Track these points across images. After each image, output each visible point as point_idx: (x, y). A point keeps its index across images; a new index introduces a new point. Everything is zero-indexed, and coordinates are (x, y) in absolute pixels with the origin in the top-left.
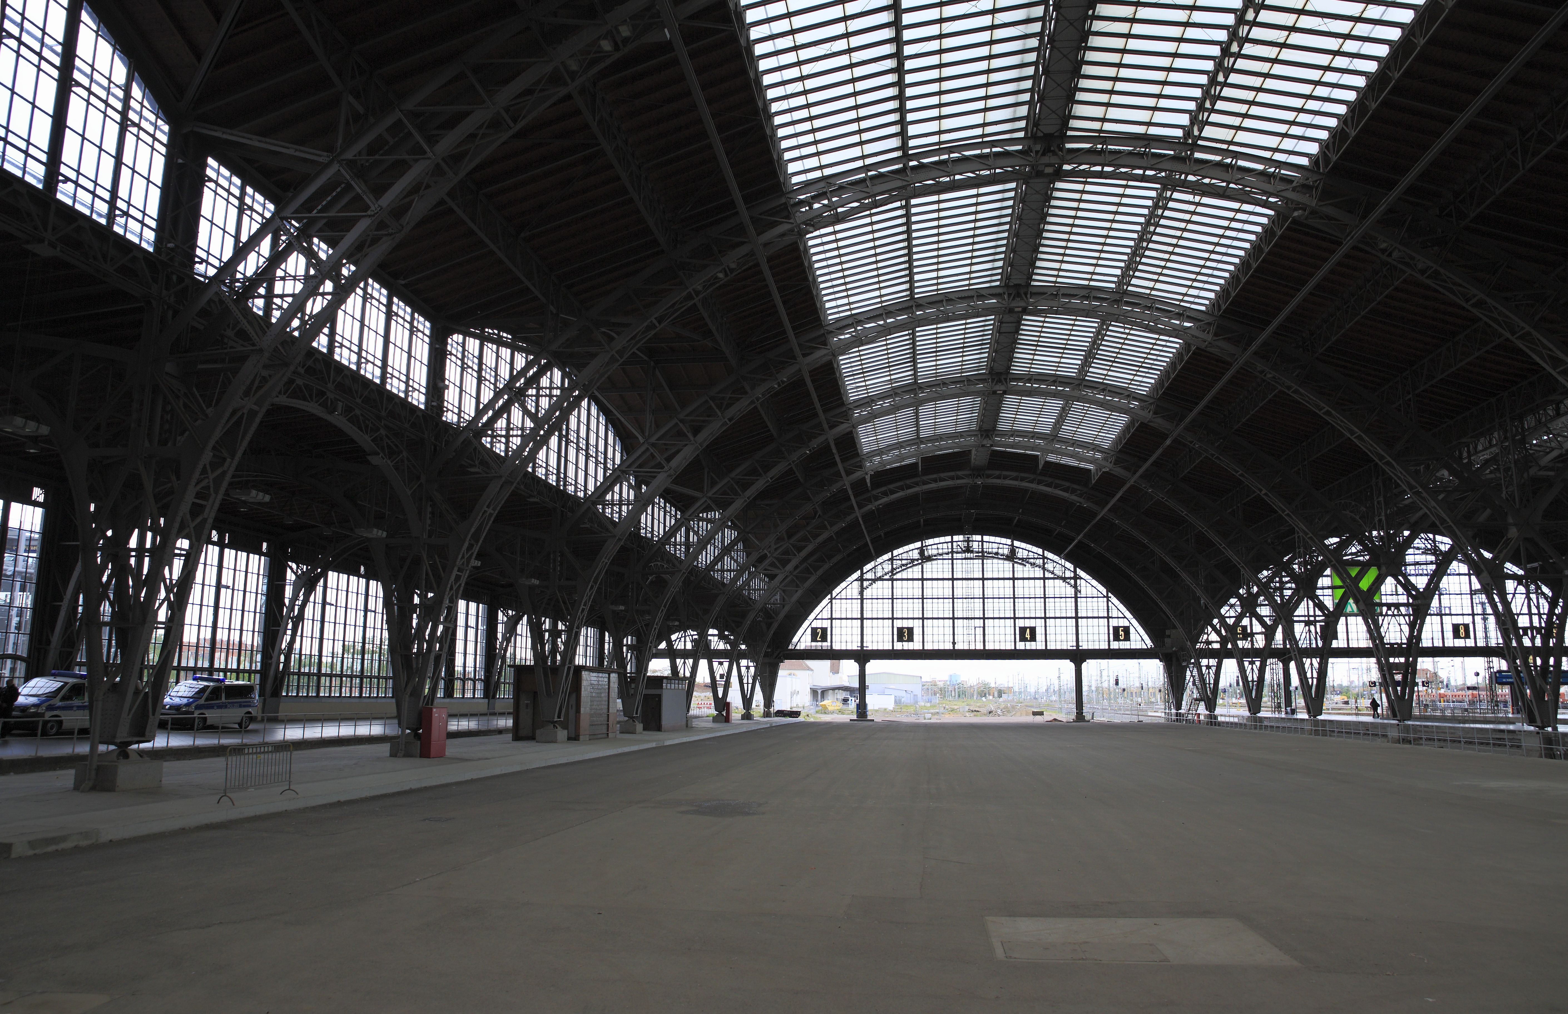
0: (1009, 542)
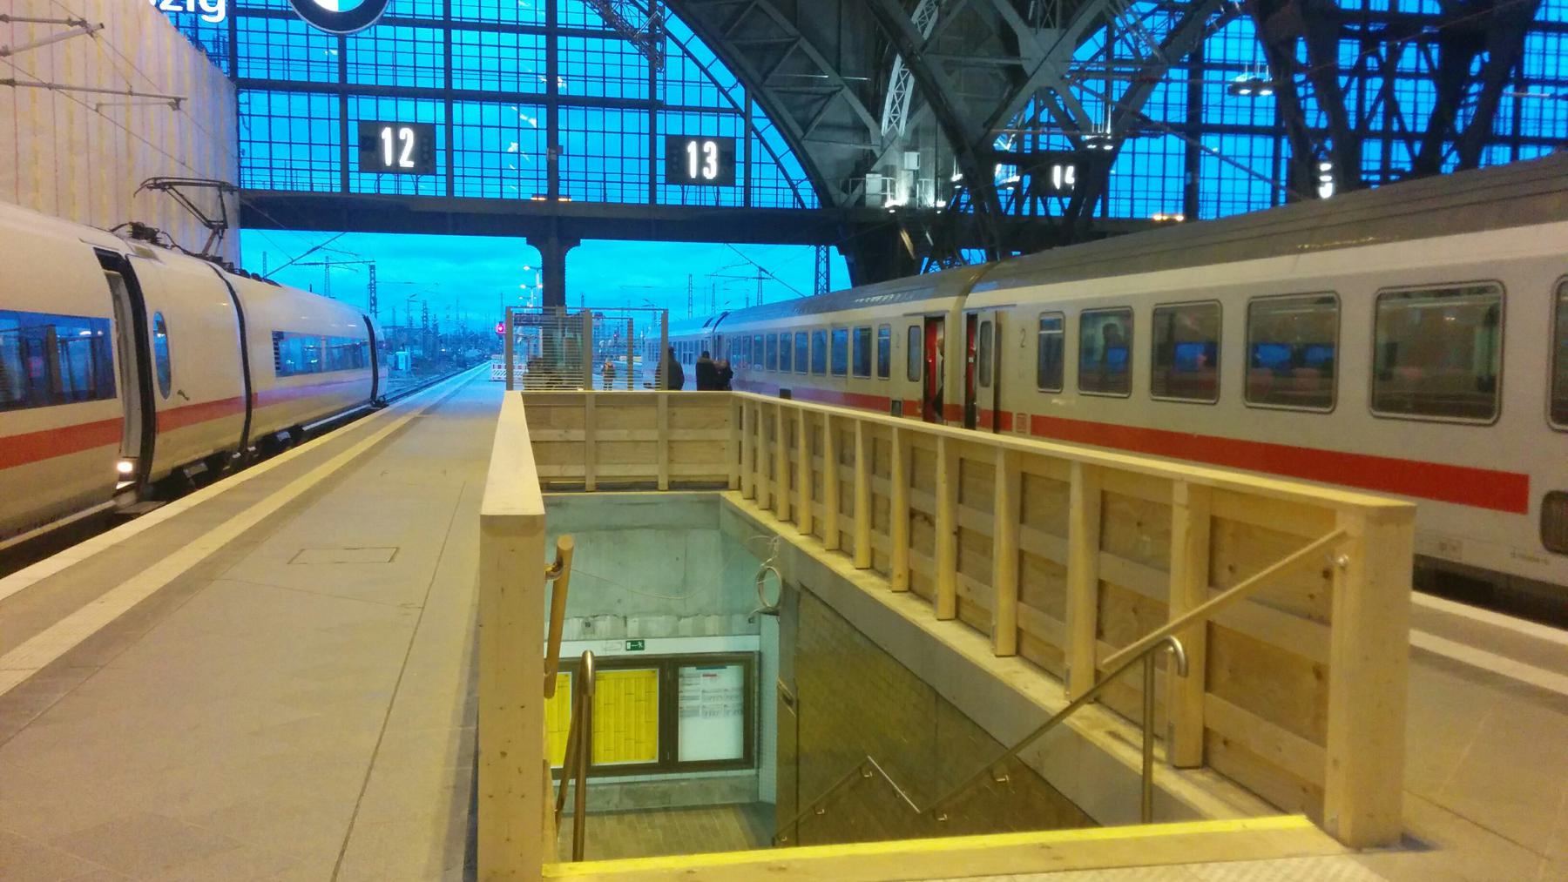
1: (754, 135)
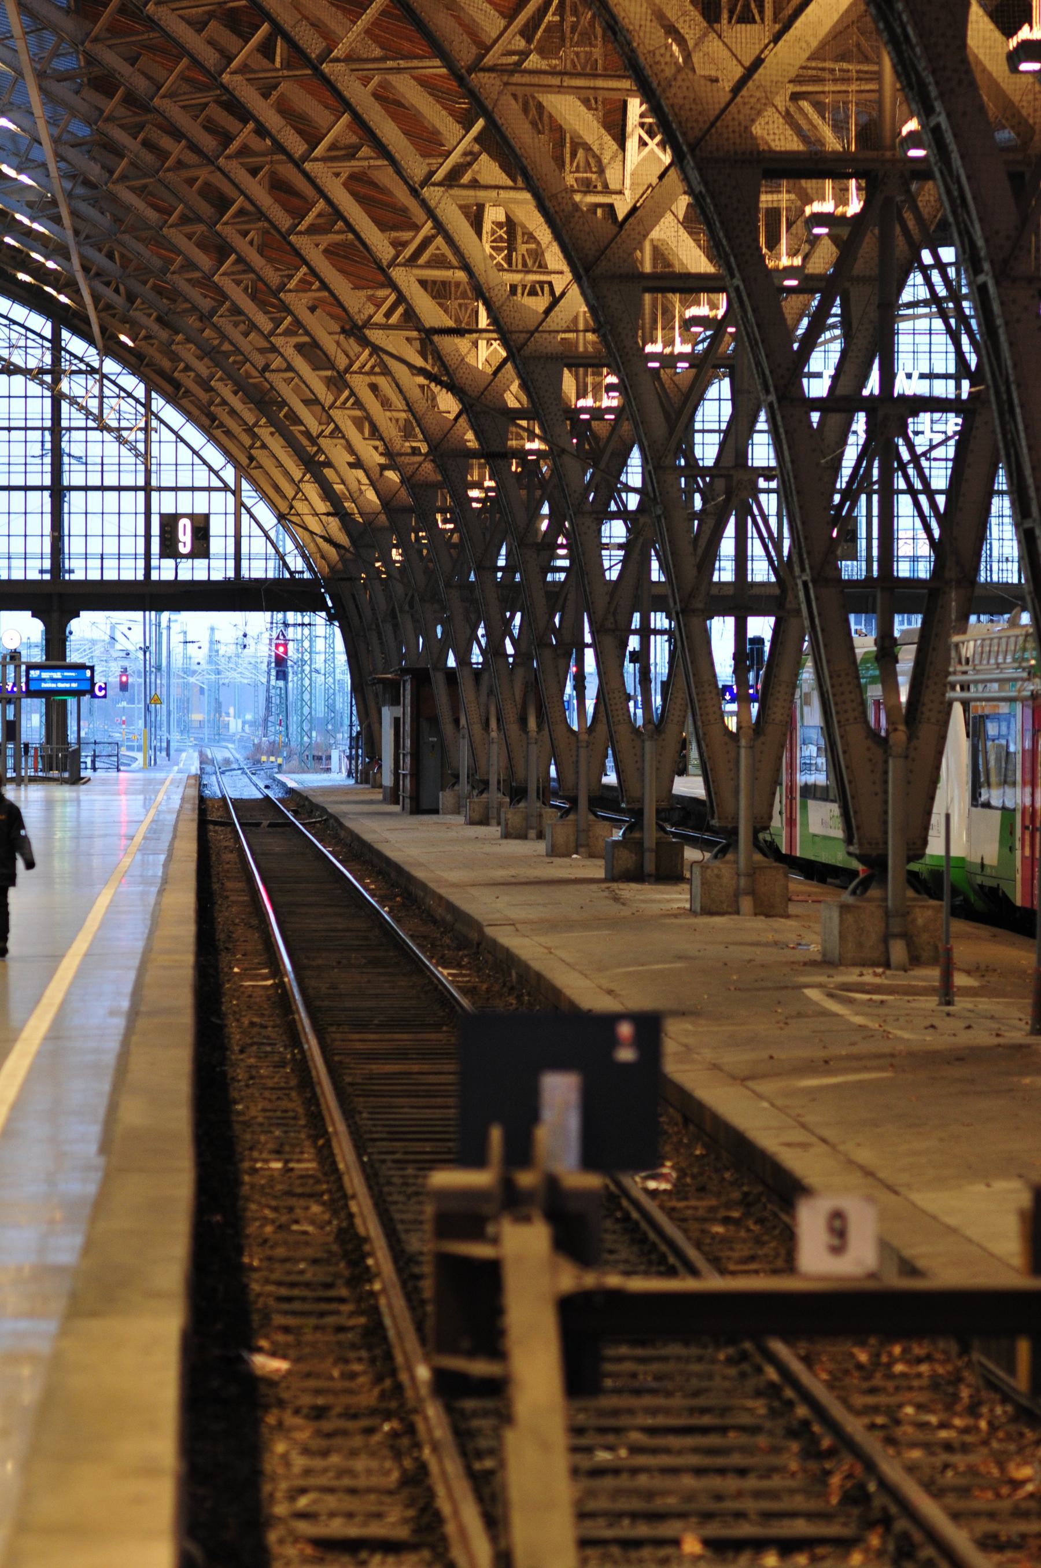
1: (243, 511)
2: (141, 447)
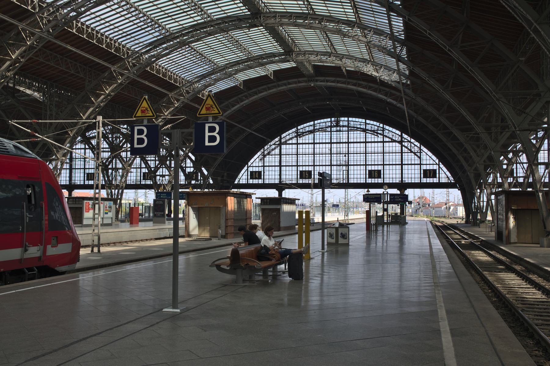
0: (364, 121)
2: (419, 156)
